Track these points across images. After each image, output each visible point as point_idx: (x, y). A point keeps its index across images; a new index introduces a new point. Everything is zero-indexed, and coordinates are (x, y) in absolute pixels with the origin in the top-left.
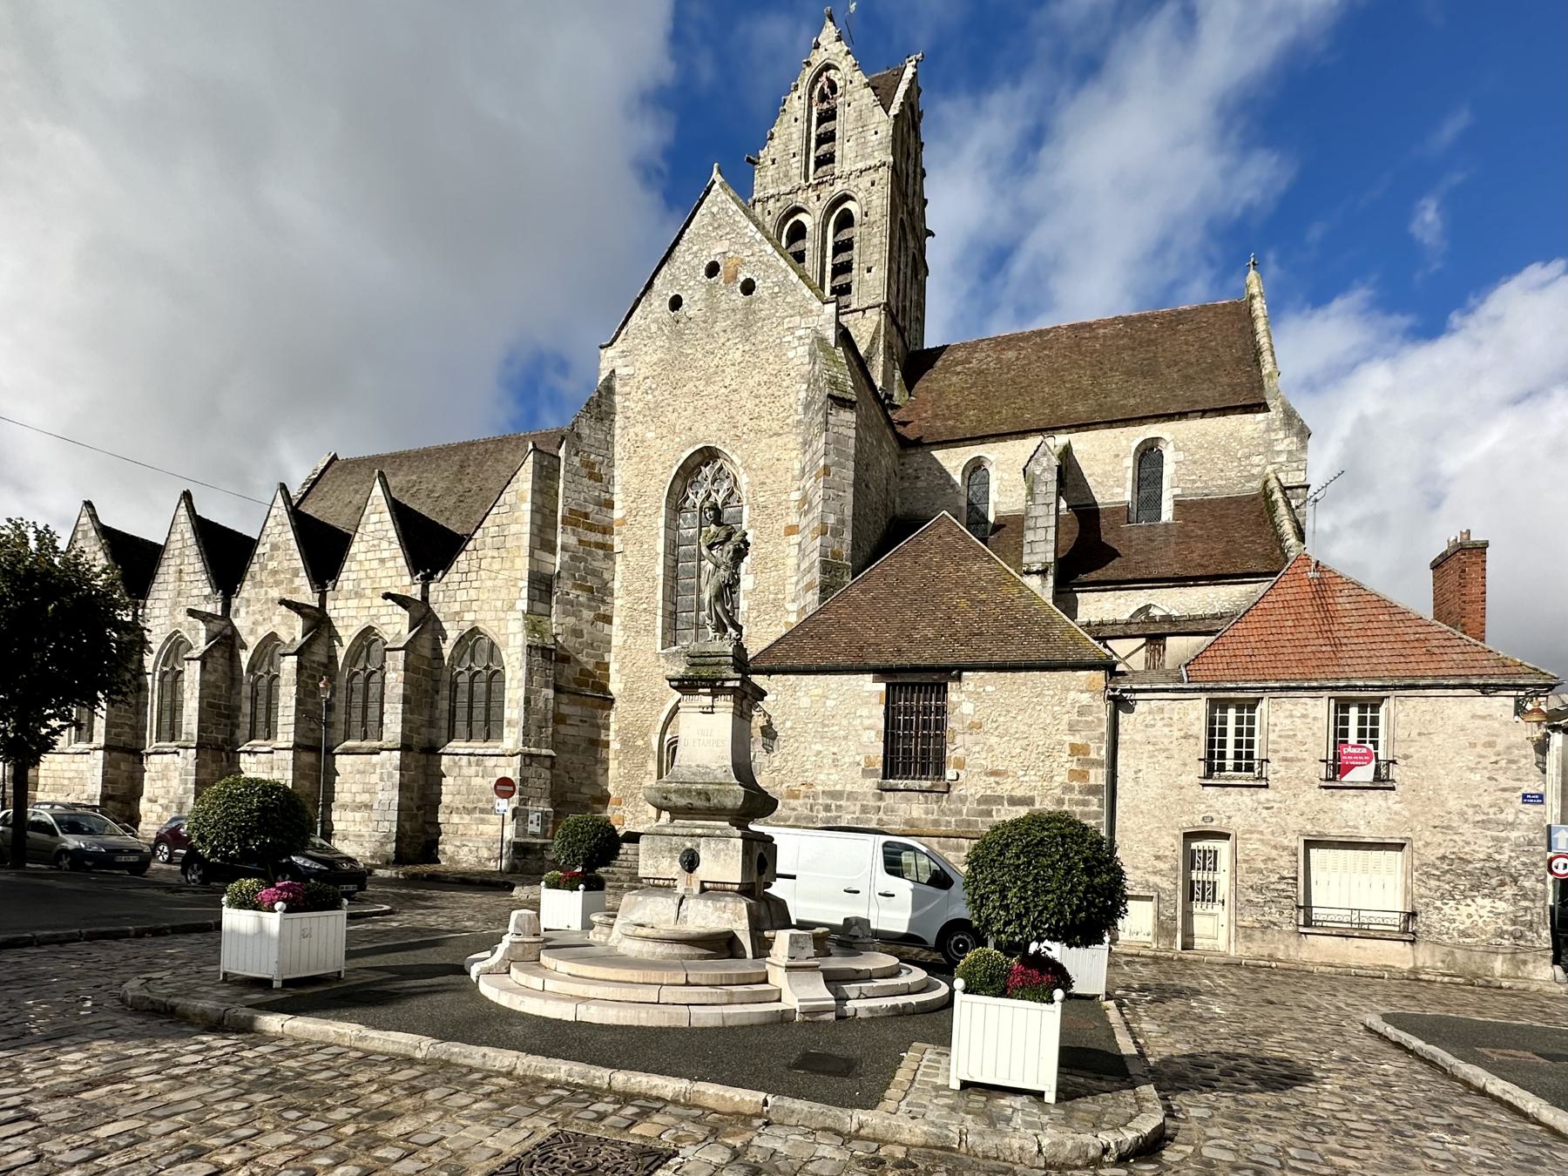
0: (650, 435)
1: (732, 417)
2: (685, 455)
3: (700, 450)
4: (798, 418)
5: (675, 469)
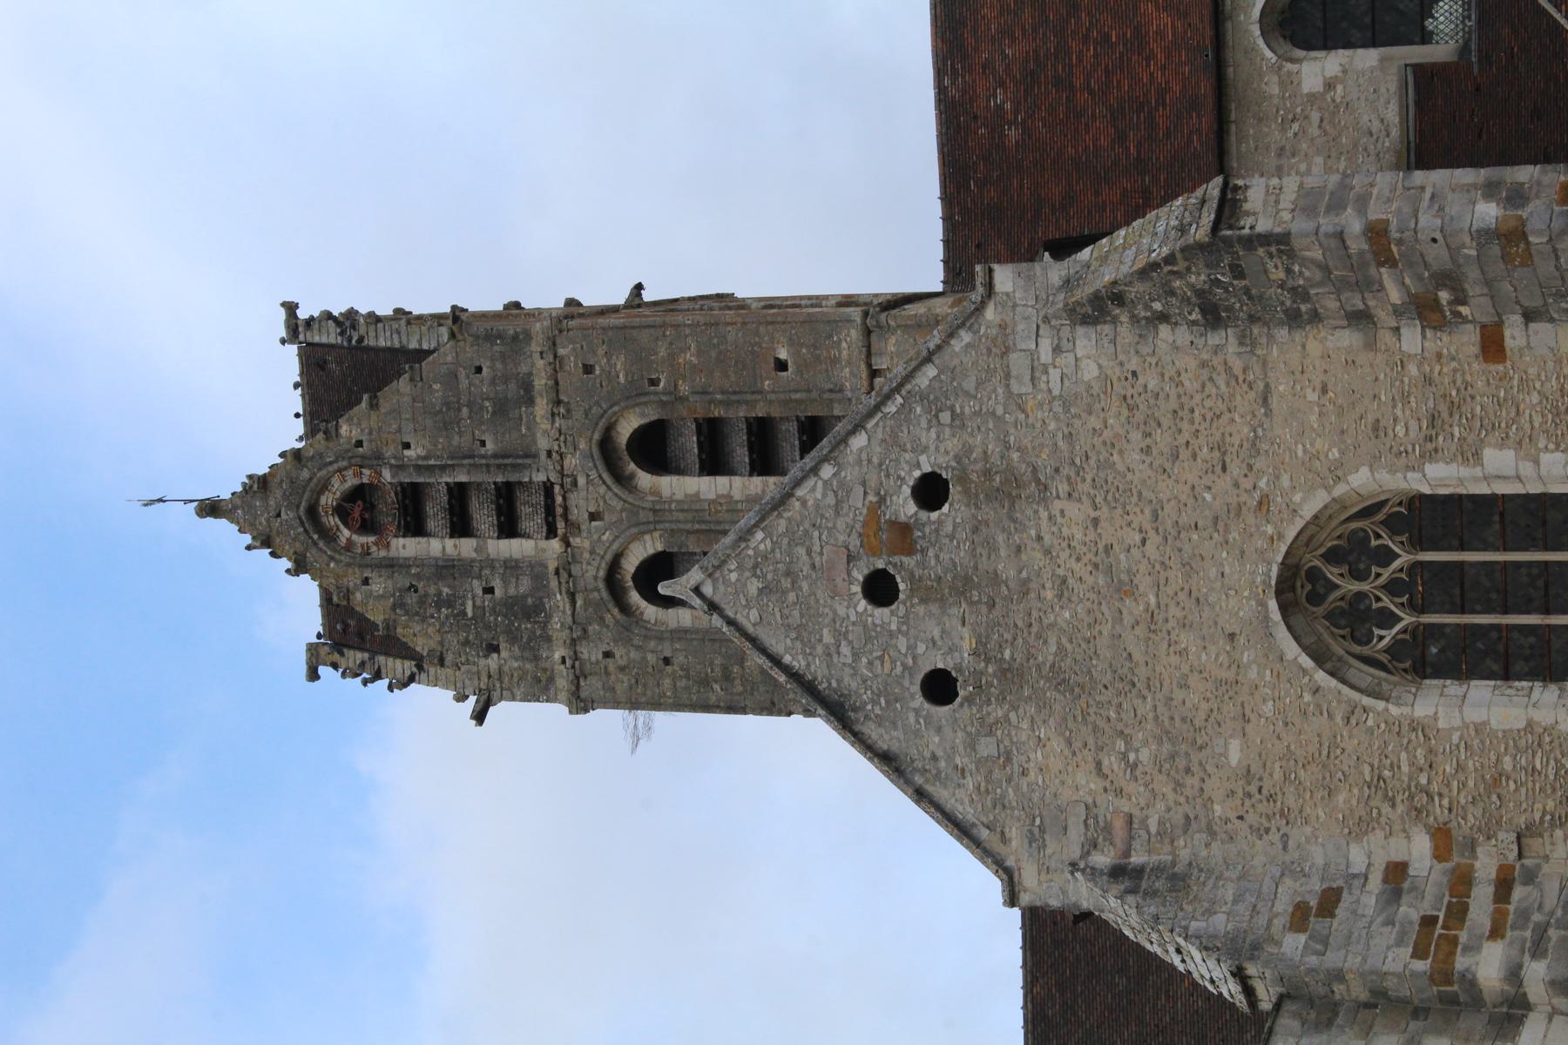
0: (1234, 756)
1: (1216, 519)
2: (1291, 648)
3: (1283, 608)
4: (1232, 347)
5: (1321, 677)
